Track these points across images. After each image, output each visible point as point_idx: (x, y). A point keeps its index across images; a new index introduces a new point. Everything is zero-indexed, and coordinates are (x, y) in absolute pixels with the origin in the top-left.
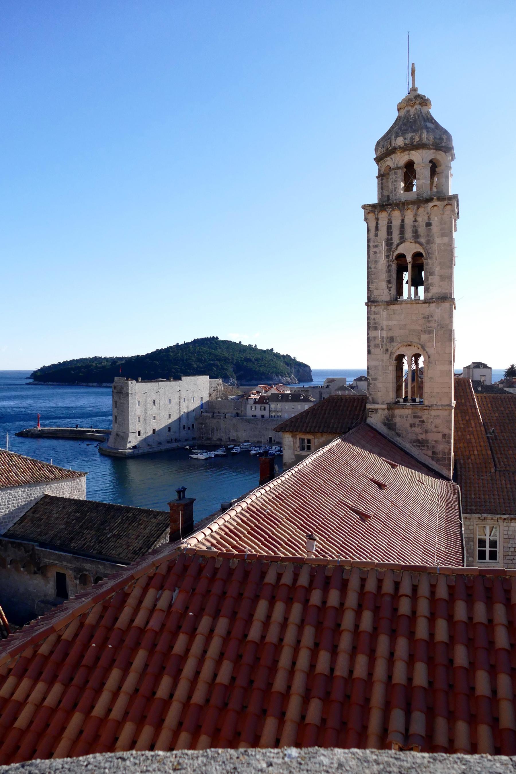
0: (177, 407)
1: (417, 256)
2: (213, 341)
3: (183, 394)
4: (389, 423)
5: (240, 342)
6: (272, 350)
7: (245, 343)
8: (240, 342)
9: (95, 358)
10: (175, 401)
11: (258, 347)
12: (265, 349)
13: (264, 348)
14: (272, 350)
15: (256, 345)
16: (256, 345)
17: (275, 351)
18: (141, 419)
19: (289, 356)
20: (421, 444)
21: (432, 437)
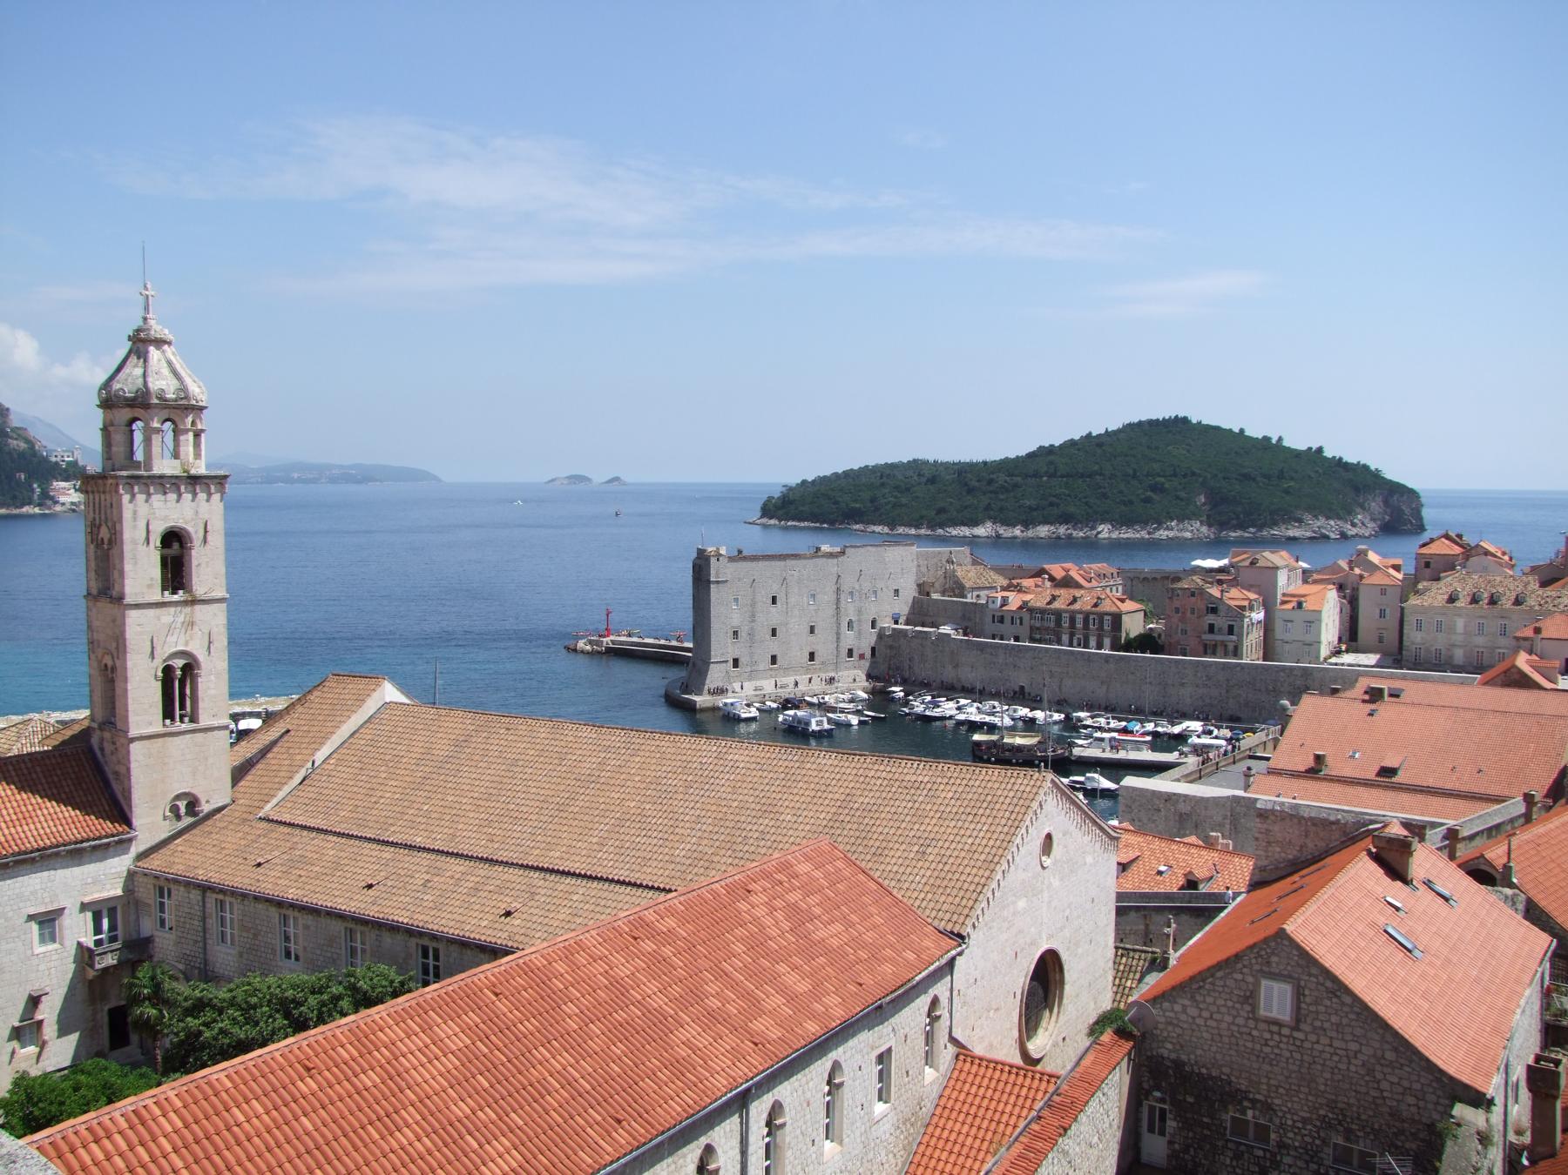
0: (831, 611)
1: (110, 542)
2: (1179, 425)
3: (848, 582)
4: (102, 749)
5: (1242, 431)
6: (1320, 450)
7: (1255, 432)
8: (1242, 431)
9: (916, 465)
10: (828, 597)
11: (1286, 443)
12: (1304, 448)
13: (1302, 447)
14: (1320, 450)
15: (1280, 439)
16: (1280, 439)
17: (1328, 453)
18: (743, 634)
19: (1366, 467)
20: (116, 773)
21: (122, 770)
